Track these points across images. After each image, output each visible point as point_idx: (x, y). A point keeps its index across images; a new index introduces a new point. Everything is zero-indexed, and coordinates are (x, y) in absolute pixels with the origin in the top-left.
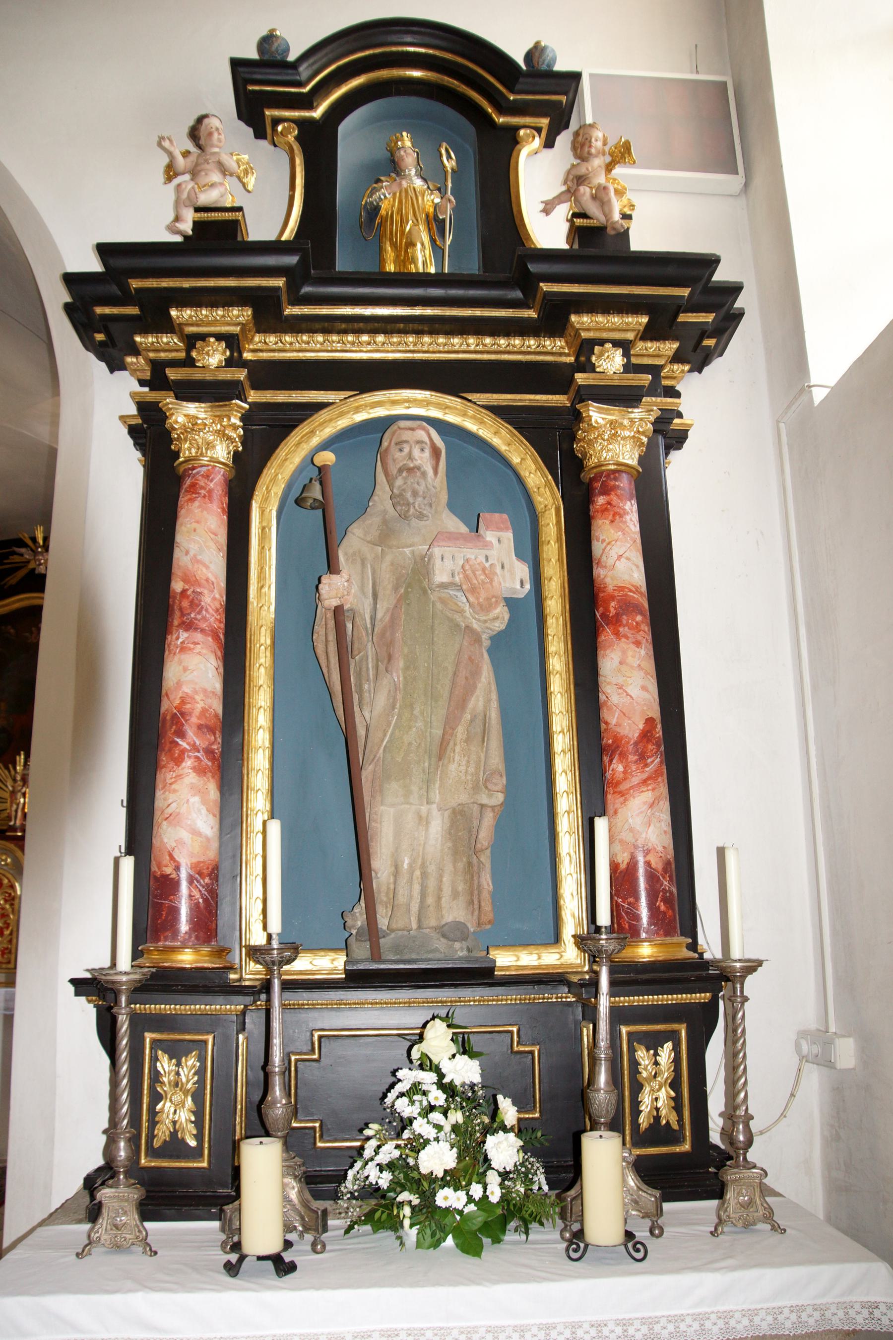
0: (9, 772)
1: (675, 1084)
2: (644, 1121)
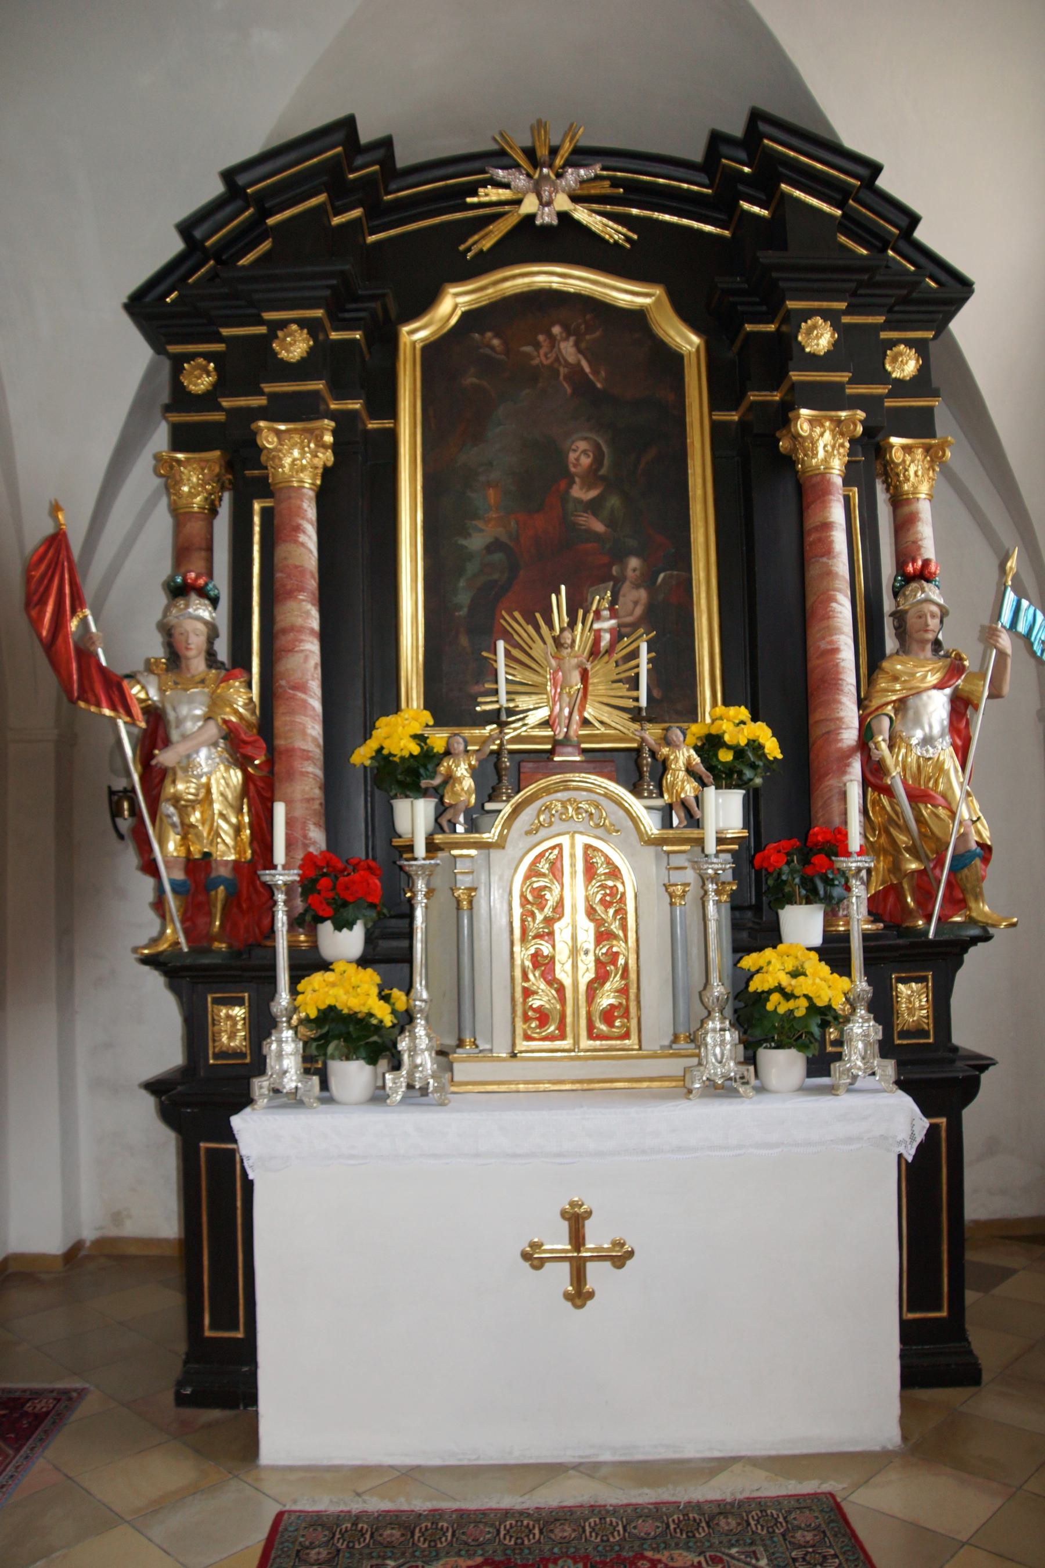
0: (537, 628)
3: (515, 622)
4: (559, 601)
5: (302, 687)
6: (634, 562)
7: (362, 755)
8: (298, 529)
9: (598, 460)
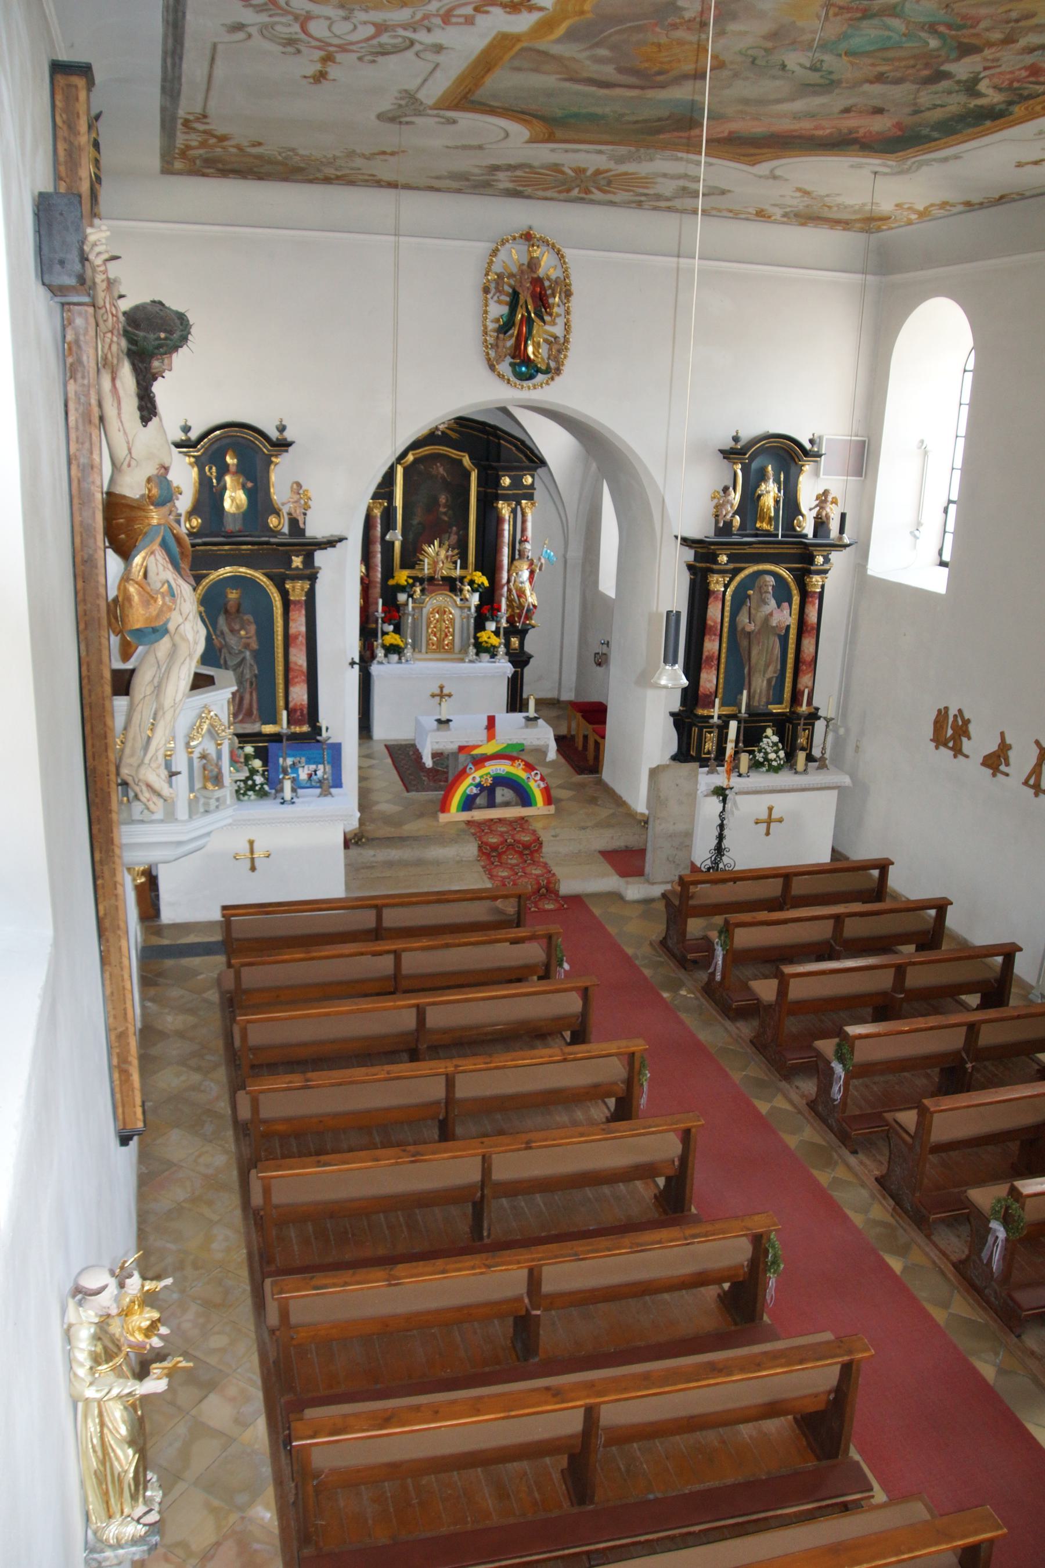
1: (808, 739)
3: (426, 548)
4: (436, 543)
5: (377, 566)
6: (454, 528)
7: (391, 582)
8: (376, 526)
9: (447, 500)
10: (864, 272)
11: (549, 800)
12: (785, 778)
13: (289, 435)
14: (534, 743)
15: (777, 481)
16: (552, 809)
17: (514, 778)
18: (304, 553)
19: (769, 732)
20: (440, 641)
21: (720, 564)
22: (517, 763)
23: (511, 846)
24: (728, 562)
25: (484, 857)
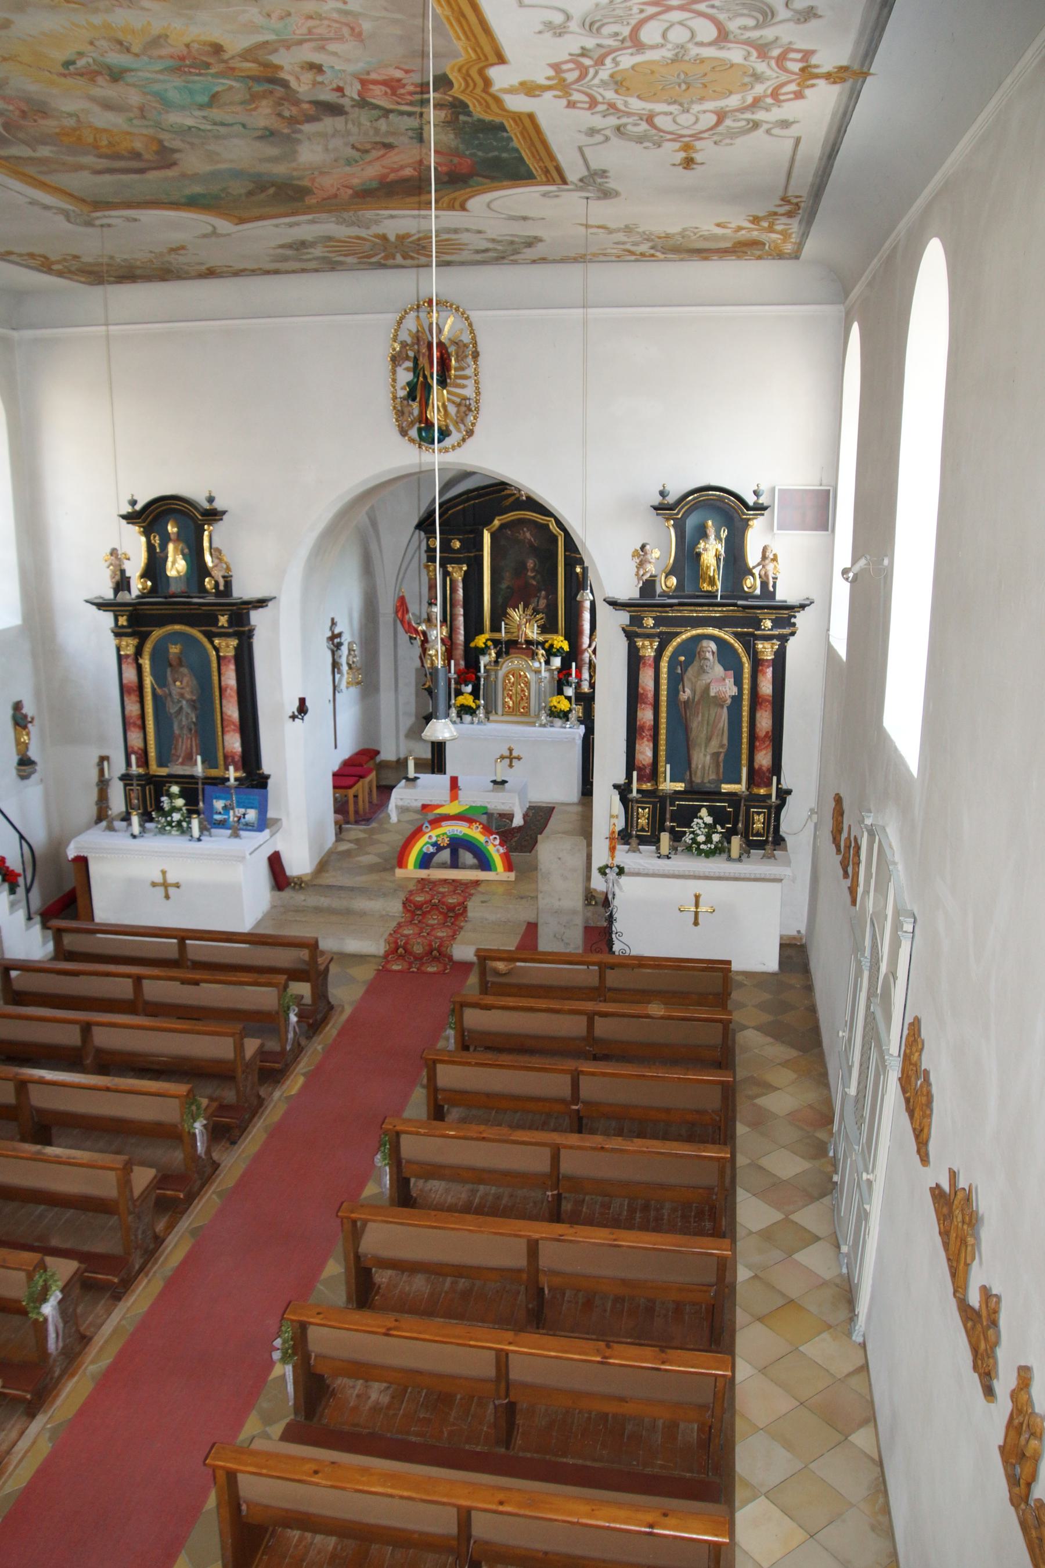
2: (754, 832)
3: (510, 611)
4: (521, 606)
5: (459, 629)
6: (543, 593)
7: (472, 645)
9: (535, 565)
10: (832, 303)
11: (509, 867)
12: (717, 865)
13: (219, 505)
14: (499, 807)
15: (718, 537)
16: (512, 876)
17: (474, 841)
18: (228, 613)
19: (704, 812)
20: (517, 704)
21: (646, 628)
22: (474, 825)
23: (435, 907)
24: (655, 626)
25: (408, 915)
